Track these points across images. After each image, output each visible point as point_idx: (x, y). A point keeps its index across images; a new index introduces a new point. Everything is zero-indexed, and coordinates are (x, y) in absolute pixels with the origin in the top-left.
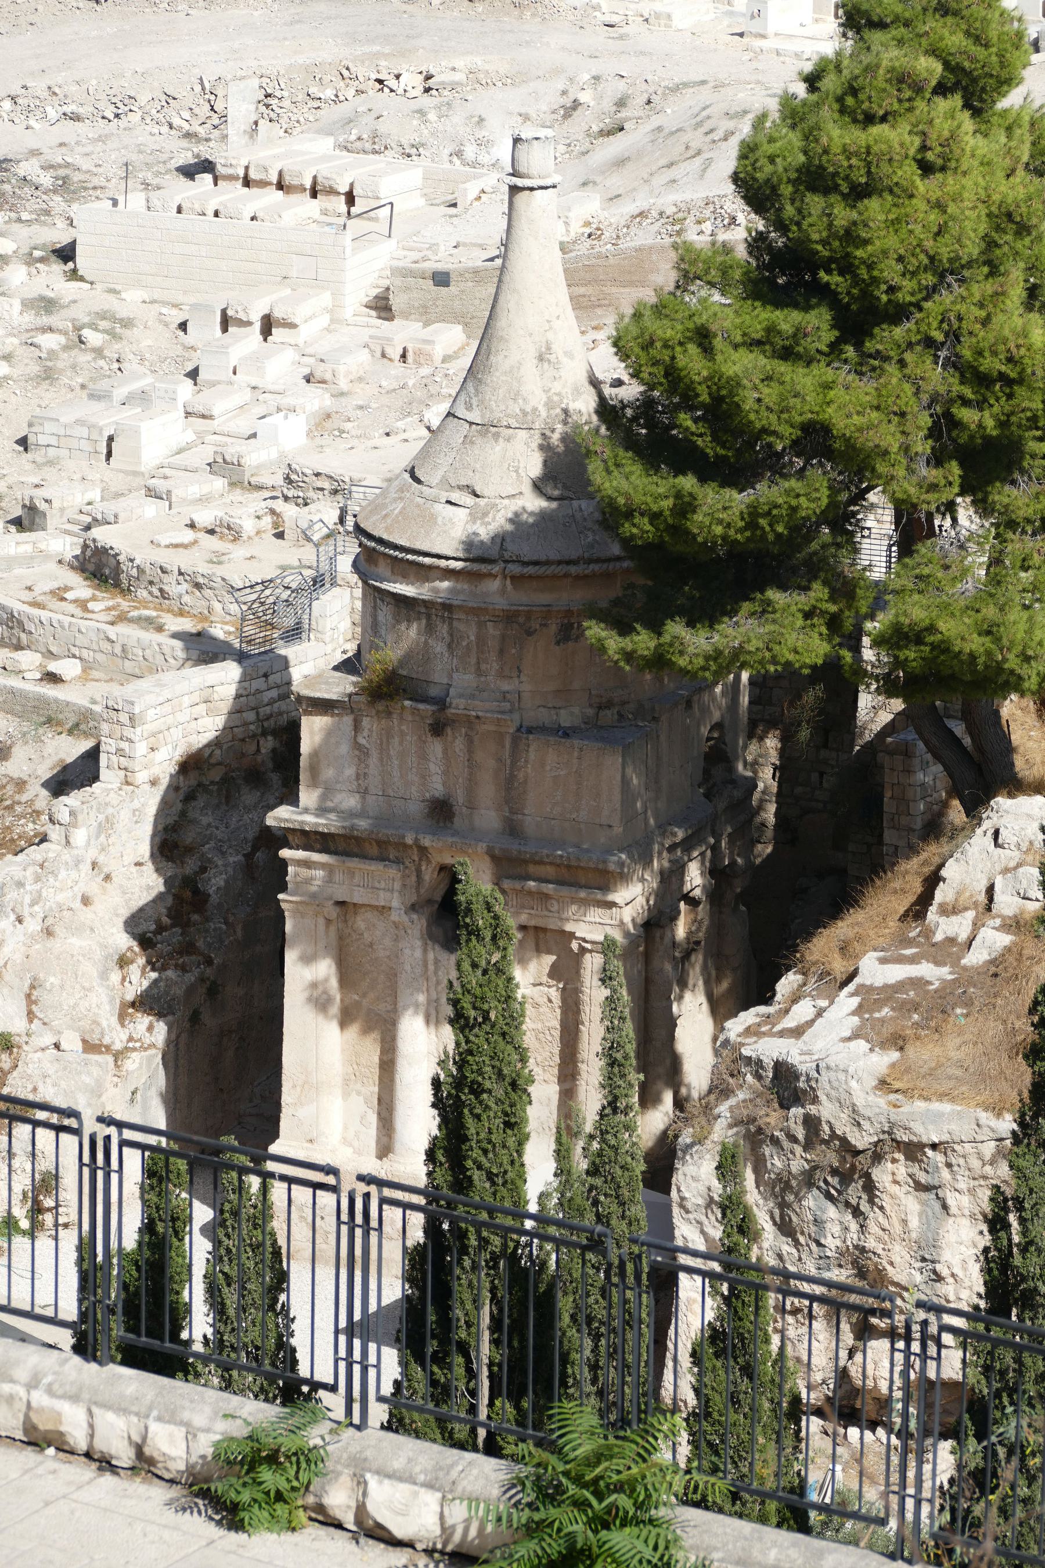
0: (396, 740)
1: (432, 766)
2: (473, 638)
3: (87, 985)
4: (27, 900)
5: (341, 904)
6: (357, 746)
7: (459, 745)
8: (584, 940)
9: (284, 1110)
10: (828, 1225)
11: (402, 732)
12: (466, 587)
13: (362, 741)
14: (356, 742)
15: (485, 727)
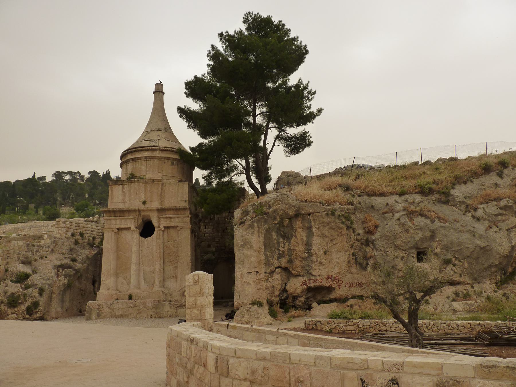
0: (133, 189)
1: (142, 194)
2: (152, 164)
3: (49, 269)
4: (35, 250)
5: (118, 229)
6: (123, 192)
7: (149, 188)
8: (181, 226)
9: (101, 282)
10: (281, 243)
11: (134, 187)
12: (150, 153)
13: (125, 191)
14: (123, 191)
15: (155, 183)
